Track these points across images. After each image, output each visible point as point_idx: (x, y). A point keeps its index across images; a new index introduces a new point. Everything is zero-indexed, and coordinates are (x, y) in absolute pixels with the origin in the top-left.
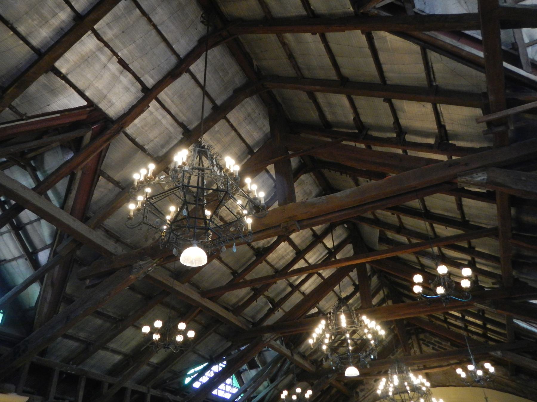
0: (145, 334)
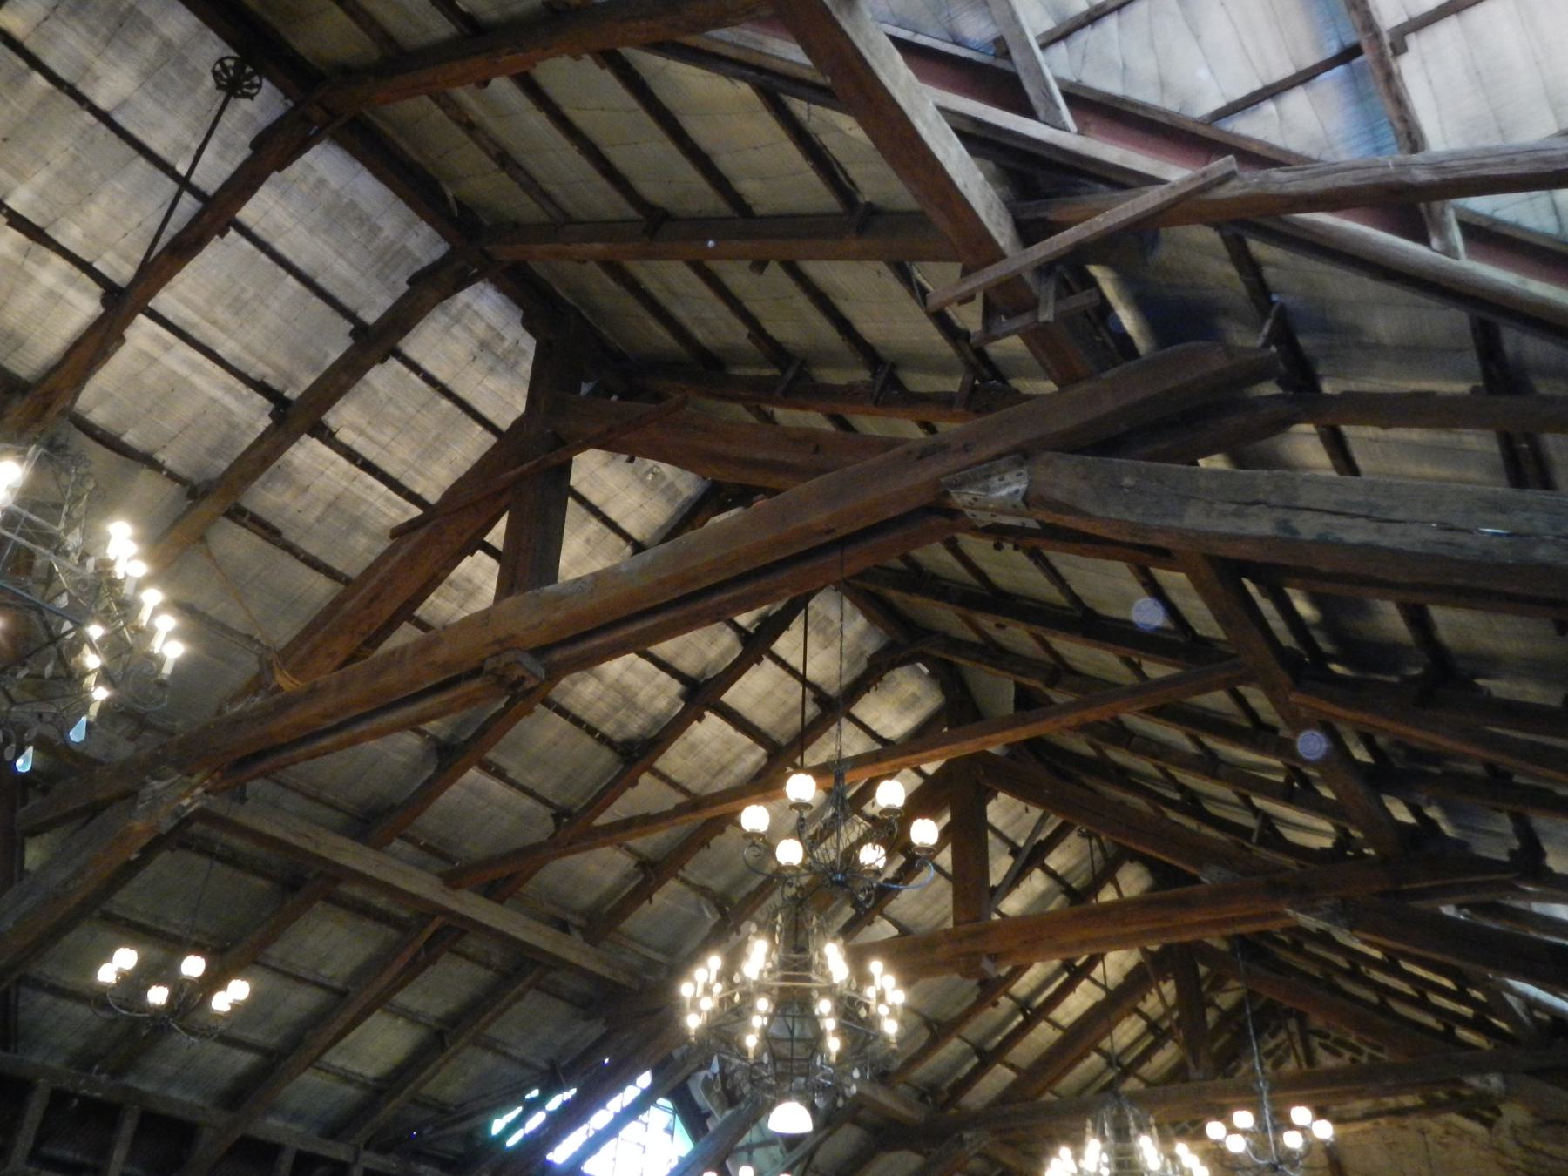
0: (160, 983)
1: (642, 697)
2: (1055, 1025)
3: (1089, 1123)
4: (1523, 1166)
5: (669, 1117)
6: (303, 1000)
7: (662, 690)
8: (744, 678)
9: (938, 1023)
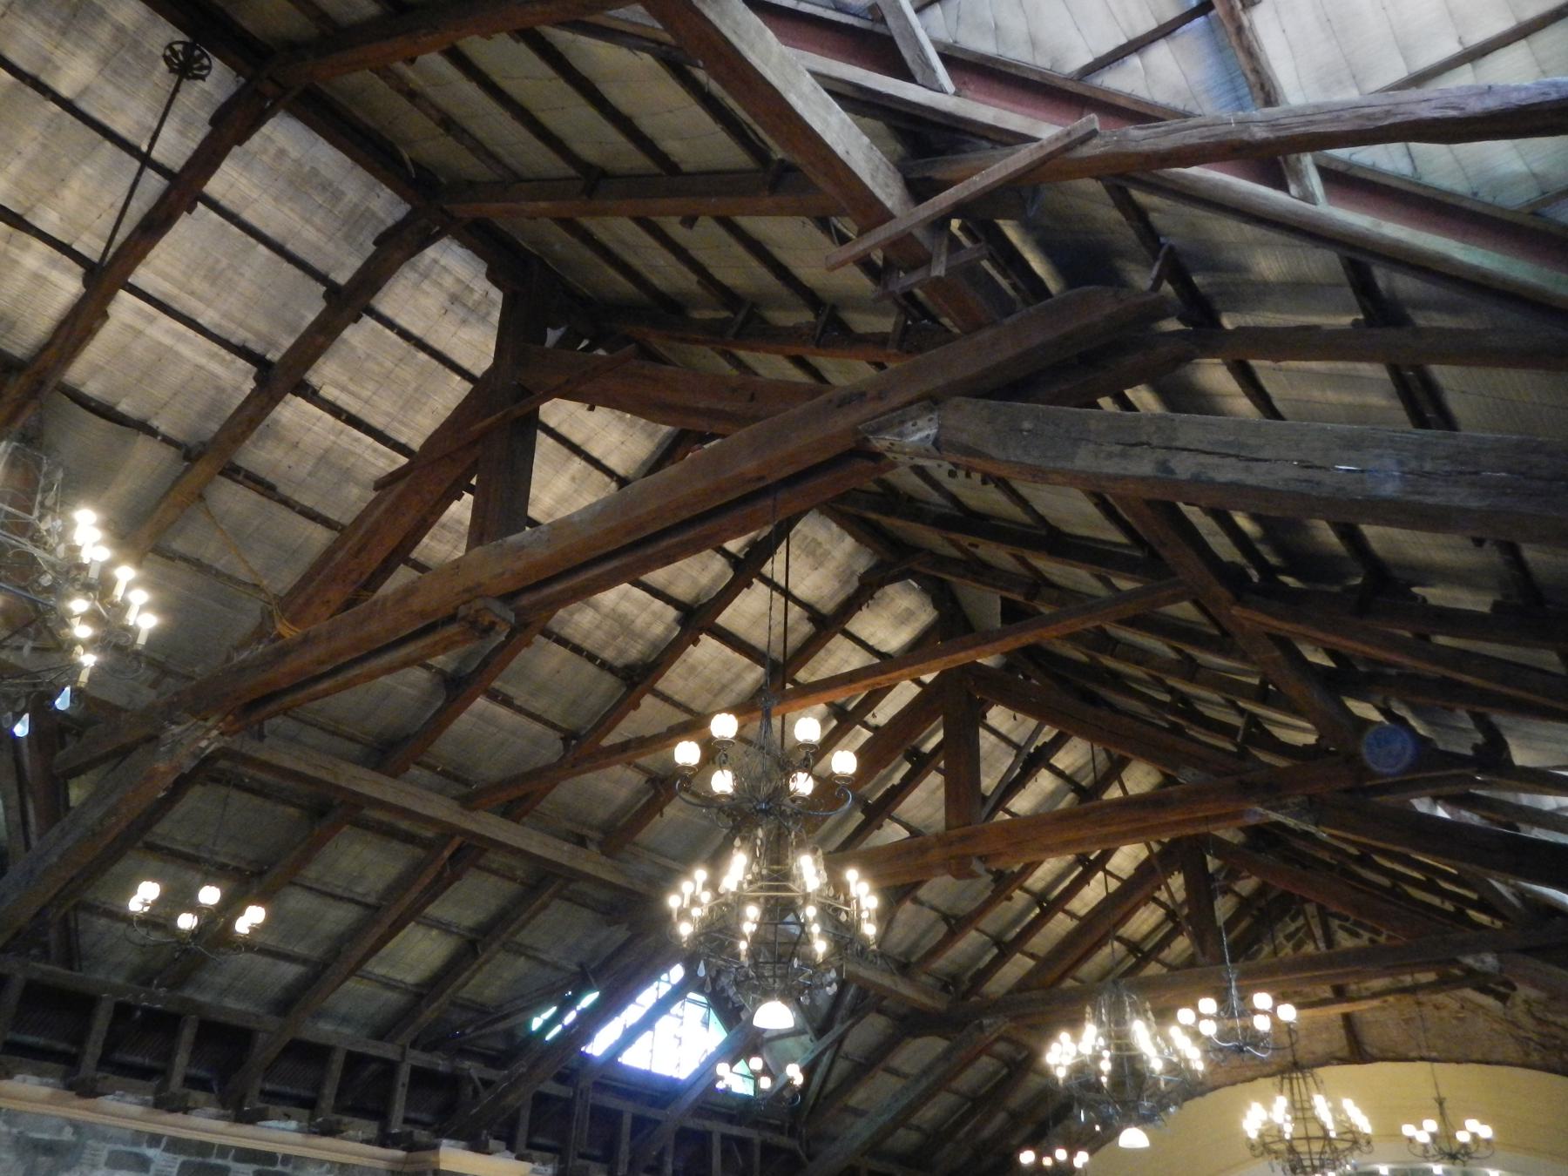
1: (640, 622)
2: (1072, 915)
3: (1088, 1009)
4: (1535, 1037)
5: (702, 1011)
6: (338, 917)
7: (658, 616)
8: (737, 601)
9: (955, 917)
